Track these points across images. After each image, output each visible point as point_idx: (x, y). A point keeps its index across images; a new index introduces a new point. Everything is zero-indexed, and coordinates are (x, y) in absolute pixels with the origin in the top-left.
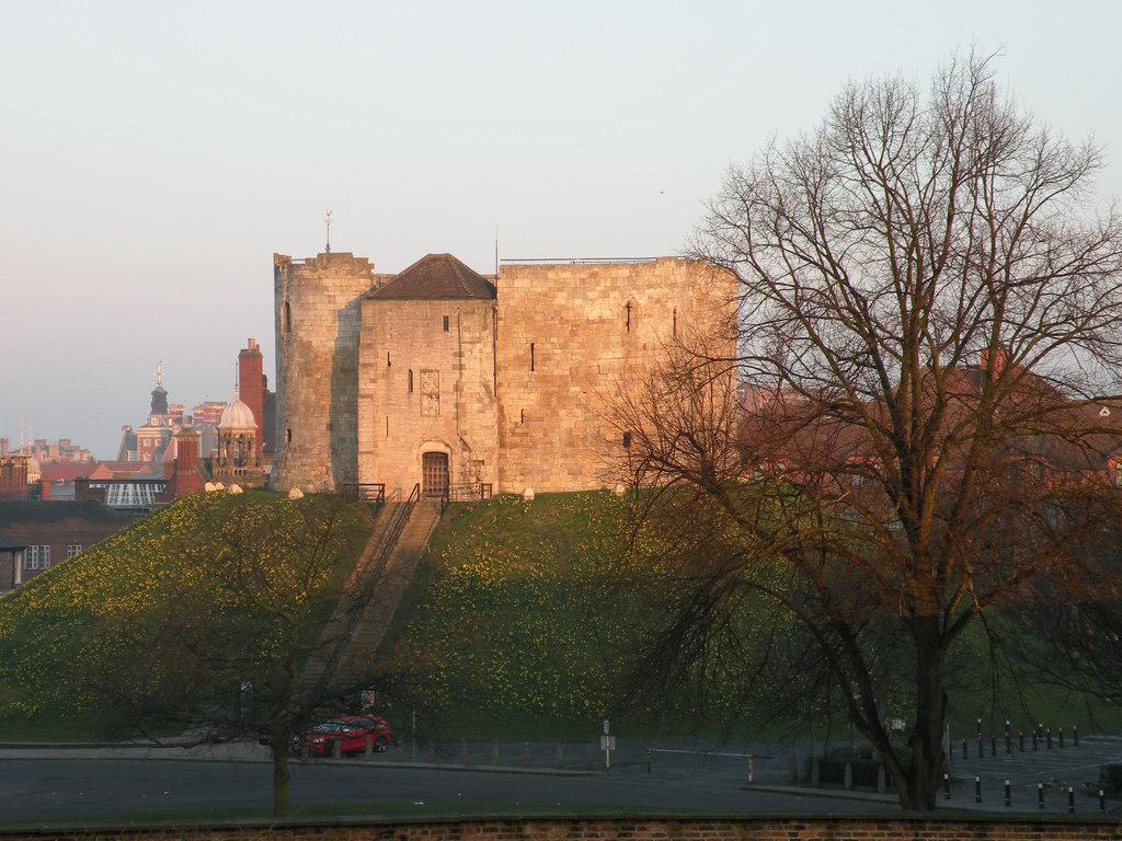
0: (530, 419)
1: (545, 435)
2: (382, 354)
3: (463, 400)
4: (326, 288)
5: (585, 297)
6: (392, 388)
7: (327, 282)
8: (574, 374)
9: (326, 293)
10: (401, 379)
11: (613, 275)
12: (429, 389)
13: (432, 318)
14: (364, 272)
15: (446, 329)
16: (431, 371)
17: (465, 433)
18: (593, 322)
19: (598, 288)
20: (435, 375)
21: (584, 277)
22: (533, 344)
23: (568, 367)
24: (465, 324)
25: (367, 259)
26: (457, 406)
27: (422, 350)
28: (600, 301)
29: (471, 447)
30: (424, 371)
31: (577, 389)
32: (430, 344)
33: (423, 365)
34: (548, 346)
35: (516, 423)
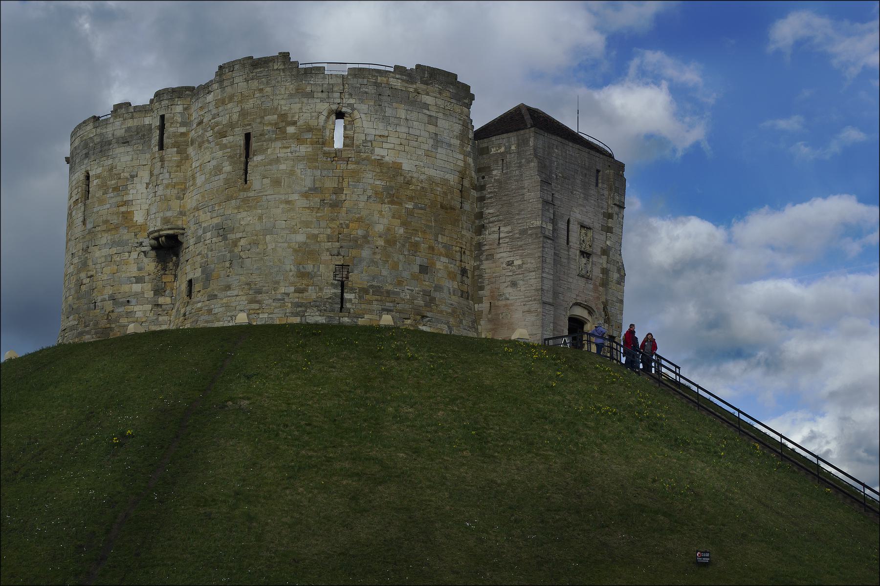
4: (426, 106)
26: (605, 271)
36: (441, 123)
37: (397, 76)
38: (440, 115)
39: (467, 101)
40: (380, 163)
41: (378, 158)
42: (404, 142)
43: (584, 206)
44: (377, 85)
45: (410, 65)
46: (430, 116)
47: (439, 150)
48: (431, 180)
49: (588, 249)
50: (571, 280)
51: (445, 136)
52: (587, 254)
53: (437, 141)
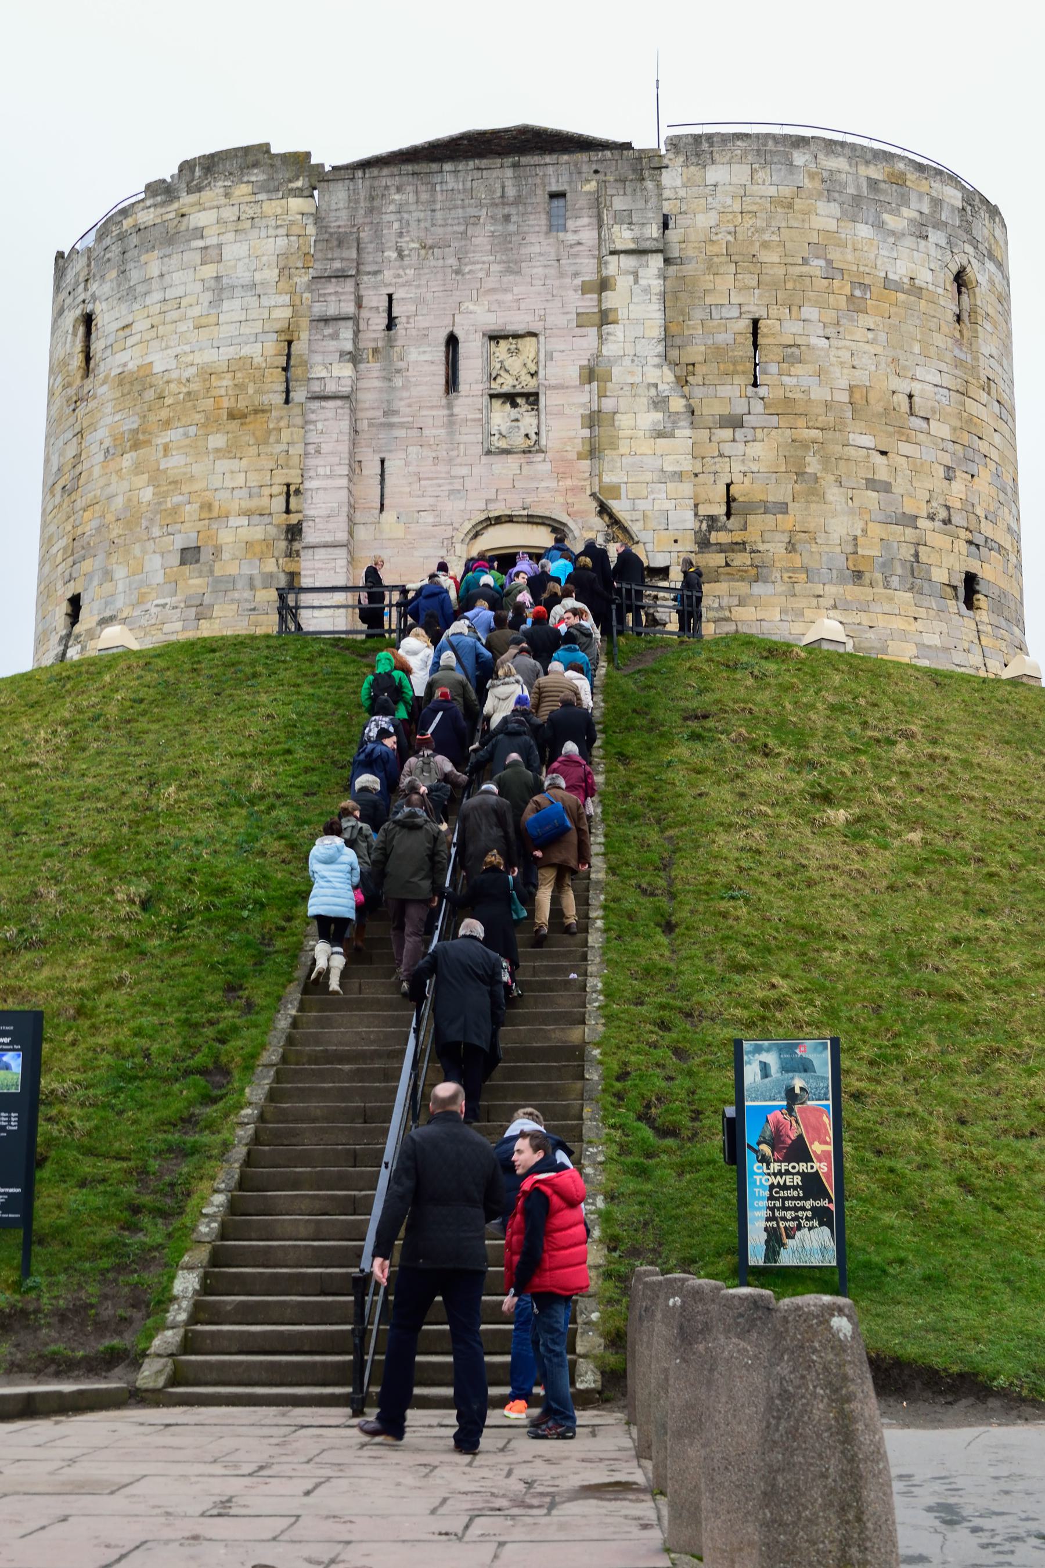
0: (750, 508)
1: (791, 547)
2: (375, 300)
3: (608, 404)
4: (199, 233)
5: (879, 225)
6: (398, 382)
7: (200, 219)
8: (858, 401)
9: (200, 243)
10: (425, 361)
11: (934, 194)
12: (506, 384)
13: (518, 201)
14: (299, 184)
15: (555, 225)
16: (516, 336)
17: (615, 491)
18: (898, 287)
19: (905, 212)
20: (528, 346)
21: (875, 175)
22: (755, 322)
23: (844, 383)
24: (619, 203)
25: (308, 155)
26: (594, 419)
27: (490, 283)
28: (909, 241)
29: (635, 528)
30: (495, 338)
31: (867, 441)
32: (513, 268)
33: (493, 322)
34: (796, 327)
35: (712, 519)
36: (235, 250)
37: (148, 203)
38: (230, 236)
39: (299, 184)
40: (122, 379)
41: (120, 370)
42: (156, 320)
43: (506, 290)
44: (122, 237)
45: (167, 171)
46: (206, 248)
47: (226, 305)
48: (208, 373)
49: (529, 384)
50: (464, 471)
51: (242, 275)
52: (526, 395)
53: (220, 289)
